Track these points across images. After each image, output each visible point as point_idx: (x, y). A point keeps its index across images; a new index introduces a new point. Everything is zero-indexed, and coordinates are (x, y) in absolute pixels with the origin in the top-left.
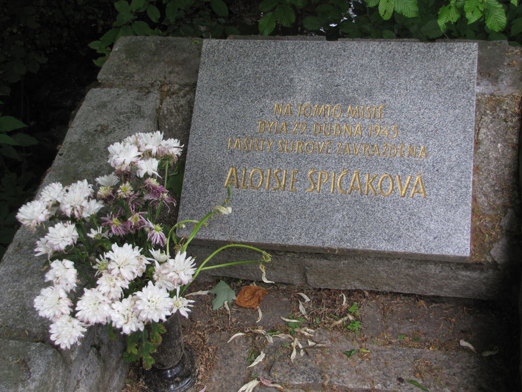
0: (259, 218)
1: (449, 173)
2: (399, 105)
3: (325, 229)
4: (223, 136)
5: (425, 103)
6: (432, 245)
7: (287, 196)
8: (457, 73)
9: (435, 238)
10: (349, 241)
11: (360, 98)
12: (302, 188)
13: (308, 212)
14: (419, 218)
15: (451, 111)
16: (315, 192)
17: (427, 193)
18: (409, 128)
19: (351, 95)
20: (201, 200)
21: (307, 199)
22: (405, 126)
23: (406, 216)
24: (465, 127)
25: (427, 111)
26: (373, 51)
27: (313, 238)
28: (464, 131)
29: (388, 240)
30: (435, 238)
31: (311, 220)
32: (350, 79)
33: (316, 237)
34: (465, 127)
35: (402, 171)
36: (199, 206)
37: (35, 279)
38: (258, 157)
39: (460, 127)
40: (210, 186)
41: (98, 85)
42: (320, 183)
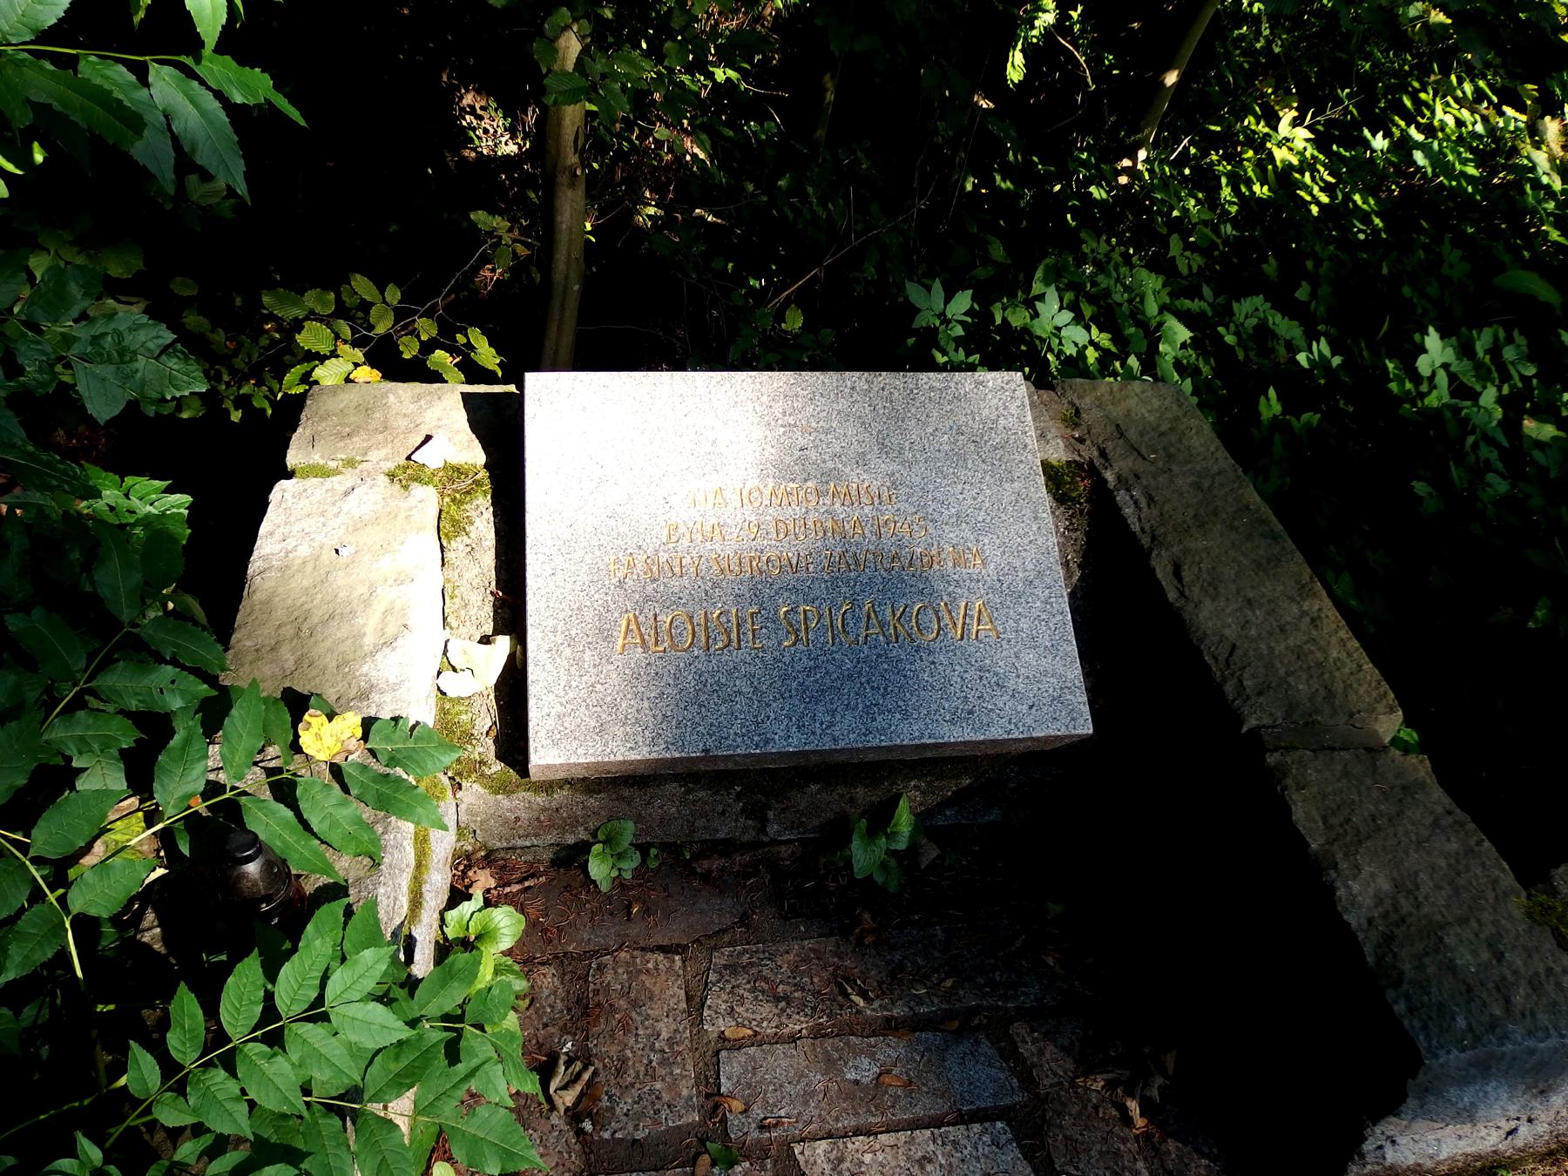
0: (700, 706)
1: (1028, 591)
2: (919, 479)
3: (833, 712)
4: (598, 553)
5: (962, 473)
6: (1029, 721)
7: (749, 659)
8: (1002, 421)
9: (1031, 707)
10: (882, 731)
11: (847, 470)
12: (774, 641)
13: (794, 685)
14: (996, 674)
15: (1006, 486)
16: (800, 646)
17: (1000, 629)
18: (945, 517)
19: (830, 465)
20: (574, 684)
21: (787, 659)
22: (936, 516)
23: (972, 673)
24: (1035, 512)
25: (967, 487)
26: (853, 388)
27: (813, 733)
28: (1036, 518)
29: (951, 721)
30: (1031, 707)
31: (802, 700)
32: (822, 436)
33: (818, 731)
34: (1035, 512)
35: (949, 595)
36: (571, 695)
37: (1543, 1117)
38: (676, 590)
39: (1029, 514)
40: (588, 652)
41: (289, 475)
42: (807, 629)
